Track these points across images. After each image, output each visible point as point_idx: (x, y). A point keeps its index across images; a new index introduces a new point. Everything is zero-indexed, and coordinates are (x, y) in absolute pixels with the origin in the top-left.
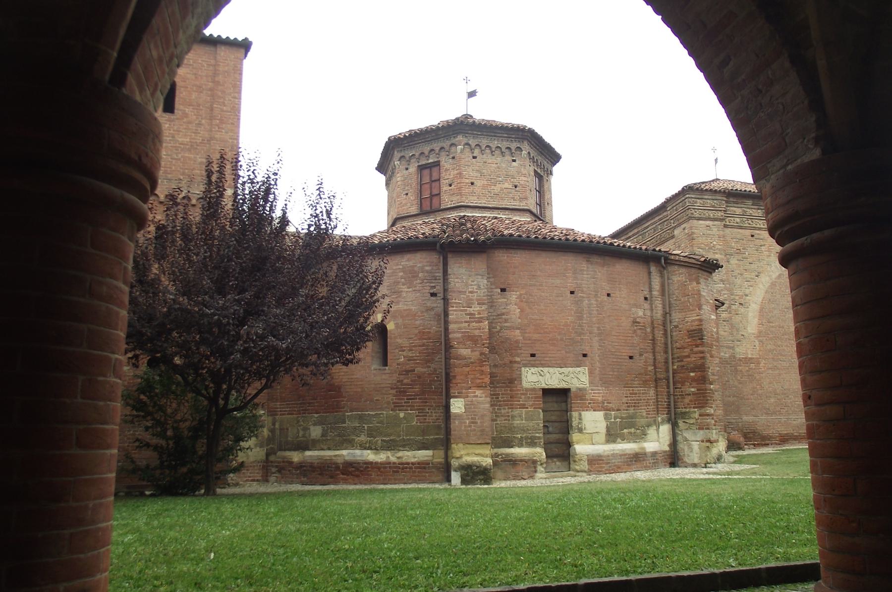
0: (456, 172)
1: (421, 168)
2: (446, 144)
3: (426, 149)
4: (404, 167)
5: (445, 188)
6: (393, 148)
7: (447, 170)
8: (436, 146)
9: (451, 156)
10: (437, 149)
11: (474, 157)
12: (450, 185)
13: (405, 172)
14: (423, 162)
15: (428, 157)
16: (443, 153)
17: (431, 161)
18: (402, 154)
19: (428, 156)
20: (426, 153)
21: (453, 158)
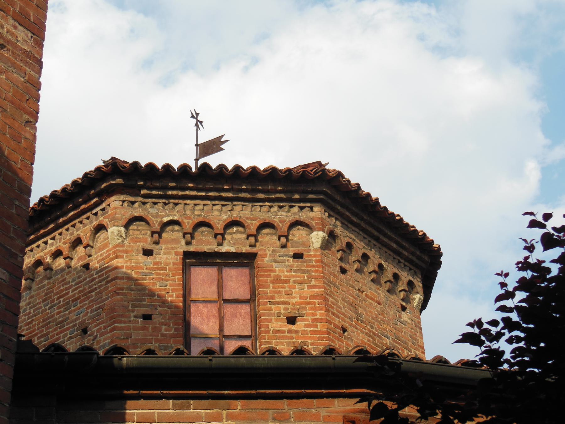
0: (307, 292)
1: (193, 259)
2: (282, 215)
3: (219, 214)
4: (141, 246)
5: (275, 325)
6: (111, 191)
7: (278, 281)
8: (251, 214)
9: (291, 250)
10: (253, 226)
11: (343, 271)
12: (291, 320)
13: (141, 258)
14: (205, 243)
15: (220, 237)
16: (268, 239)
17: (225, 249)
18: (138, 211)
19: (223, 235)
20: (219, 227)
21: (298, 256)
